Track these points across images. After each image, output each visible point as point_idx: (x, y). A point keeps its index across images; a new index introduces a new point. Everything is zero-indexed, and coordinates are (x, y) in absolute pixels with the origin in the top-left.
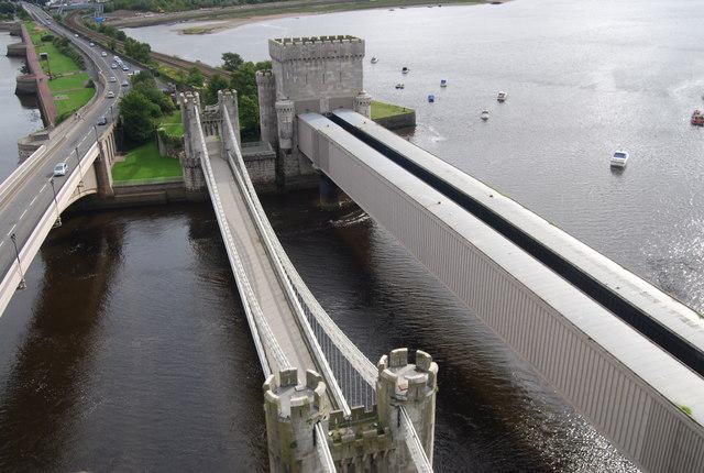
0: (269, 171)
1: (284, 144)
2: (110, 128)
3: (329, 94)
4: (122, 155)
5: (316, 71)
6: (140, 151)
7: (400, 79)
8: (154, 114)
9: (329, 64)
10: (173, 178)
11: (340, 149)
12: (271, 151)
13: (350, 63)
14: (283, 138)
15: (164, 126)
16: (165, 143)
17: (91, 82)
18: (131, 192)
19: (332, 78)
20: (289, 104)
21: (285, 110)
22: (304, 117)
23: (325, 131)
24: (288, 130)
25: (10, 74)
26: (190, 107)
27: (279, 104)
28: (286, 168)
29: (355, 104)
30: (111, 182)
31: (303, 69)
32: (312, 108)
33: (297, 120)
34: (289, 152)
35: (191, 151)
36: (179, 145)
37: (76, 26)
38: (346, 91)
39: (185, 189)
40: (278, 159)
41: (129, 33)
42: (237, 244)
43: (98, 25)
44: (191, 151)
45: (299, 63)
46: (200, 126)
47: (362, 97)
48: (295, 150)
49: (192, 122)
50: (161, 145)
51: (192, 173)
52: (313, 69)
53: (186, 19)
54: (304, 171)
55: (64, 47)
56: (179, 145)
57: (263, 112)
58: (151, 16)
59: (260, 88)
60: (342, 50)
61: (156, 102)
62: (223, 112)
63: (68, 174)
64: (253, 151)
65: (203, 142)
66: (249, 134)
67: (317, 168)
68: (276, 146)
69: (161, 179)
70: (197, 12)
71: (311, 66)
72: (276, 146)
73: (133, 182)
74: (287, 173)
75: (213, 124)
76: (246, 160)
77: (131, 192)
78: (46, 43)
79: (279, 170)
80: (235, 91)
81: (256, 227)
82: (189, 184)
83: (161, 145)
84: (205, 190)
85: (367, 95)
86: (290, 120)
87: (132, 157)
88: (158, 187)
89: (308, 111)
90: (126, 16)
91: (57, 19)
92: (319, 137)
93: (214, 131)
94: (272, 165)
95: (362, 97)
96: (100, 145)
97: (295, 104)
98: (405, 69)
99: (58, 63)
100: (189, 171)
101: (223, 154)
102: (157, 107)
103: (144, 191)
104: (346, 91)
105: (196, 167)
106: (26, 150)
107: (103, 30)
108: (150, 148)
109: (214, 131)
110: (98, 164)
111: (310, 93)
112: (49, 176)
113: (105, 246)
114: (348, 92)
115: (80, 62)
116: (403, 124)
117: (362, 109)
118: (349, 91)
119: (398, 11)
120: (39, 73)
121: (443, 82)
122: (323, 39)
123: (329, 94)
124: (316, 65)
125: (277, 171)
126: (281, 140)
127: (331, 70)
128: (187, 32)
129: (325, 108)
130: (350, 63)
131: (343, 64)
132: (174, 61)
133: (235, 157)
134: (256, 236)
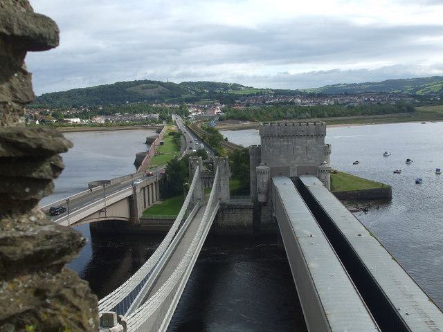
5: (288, 145)
7: (402, 166)
18: (151, 224)
19: (300, 151)
21: (262, 173)
24: (264, 188)
29: (317, 172)
30: (140, 215)
32: (283, 173)
33: (270, 185)
34: (265, 204)
38: (311, 161)
40: (258, 208)
52: (286, 143)
58: (248, 123)
59: (251, 157)
68: (256, 198)
71: (284, 141)
74: (262, 220)
75: (207, 179)
77: (151, 224)
79: (257, 217)
86: (265, 181)
87: (167, 202)
89: (280, 175)
90: (230, 123)
94: (251, 213)
95: (322, 166)
96: (134, 189)
98: (408, 160)
103: (159, 224)
104: (311, 161)
110: (131, 200)
111: (282, 161)
117: (323, 176)
118: (314, 161)
119: (429, 124)
121: (438, 170)
124: (288, 141)
131: (309, 141)
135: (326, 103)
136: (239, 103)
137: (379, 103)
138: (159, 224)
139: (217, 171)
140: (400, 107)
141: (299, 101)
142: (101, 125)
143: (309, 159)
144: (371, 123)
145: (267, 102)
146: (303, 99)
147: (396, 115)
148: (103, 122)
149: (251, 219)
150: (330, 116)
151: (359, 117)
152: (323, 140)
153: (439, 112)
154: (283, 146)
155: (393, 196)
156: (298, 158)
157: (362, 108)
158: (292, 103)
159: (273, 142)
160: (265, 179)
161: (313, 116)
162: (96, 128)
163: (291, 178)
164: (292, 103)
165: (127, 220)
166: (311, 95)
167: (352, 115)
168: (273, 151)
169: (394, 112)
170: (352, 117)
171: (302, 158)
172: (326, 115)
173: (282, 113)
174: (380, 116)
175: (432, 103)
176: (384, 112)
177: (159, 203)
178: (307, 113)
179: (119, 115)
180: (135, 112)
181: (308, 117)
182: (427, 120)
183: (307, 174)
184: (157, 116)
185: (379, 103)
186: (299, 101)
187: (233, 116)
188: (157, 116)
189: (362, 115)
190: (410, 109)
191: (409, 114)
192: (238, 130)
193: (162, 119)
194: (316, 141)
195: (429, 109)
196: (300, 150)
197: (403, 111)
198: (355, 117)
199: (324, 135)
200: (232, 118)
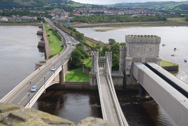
0: (120, 82)
1: (127, 73)
2: (67, 61)
3: (145, 56)
4: (70, 71)
5: (142, 47)
6: (76, 70)
8: (82, 58)
9: (147, 45)
10: (86, 81)
11: (148, 76)
12: (122, 75)
13: (154, 45)
14: (127, 70)
15: (85, 62)
16: (85, 68)
17: (63, 45)
18: (71, 84)
20: (131, 58)
21: (129, 60)
22: (135, 64)
23: (143, 69)
24: (129, 68)
25: (37, 40)
26: (95, 56)
27: (127, 58)
28: (127, 82)
29: (155, 60)
30: (64, 80)
31: (137, 46)
32: (139, 60)
34: (129, 76)
35: (93, 72)
36: (89, 69)
37: (60, 26)
39: (90, 85)
40: (125, 78)
41: (78, 30)
42: (105, 106)
43: (67, 26)
44: (93, 72)
45: (136, 44)
46: (98, 64)
47: (158, 58)
48: (131, 75)
49: (95, 62)
50: (83, 69)
51: (93, 80)
52: (141, 46)
53: (98, 26)
54: (134, 83)
55: (55, 33)
56: (89, 69)
57: (121, 60)
58: (86, 24)
59: (121, 52)
60: (152, 40)
61: (83, 54)
62: (106, 59)
63: (37, 90)
64: (115, 74)
65: (98, 69)
66: (115, 68)
67: (139, 83)
68: (124, 73)
69: (81, 81)
70: (103, 24)
71: (140, 45)
72: (124, 73)
73: (72, 81)
74: (127, 83)
75: (102, 63)
76: (113, 77)
77: (71, 84)
78: (50, 31)
79: (124, 82)
80: (111, 52)
81: (114, 102)
82: (91, 84)
83: (83, 69)
84: (97, 86)
85: (160, 58)
86: (130, 64)
87: (72, 72)
88: (81, 84)
89: (137, 61)
91: (55, 23)
92: (140, 71)
93: (102, 66)
94: (122, 80)
95: (158, 58)
96: (62, 67)
97: (133, 58)
98: (175, 49)
99: (53, 38)
100: (92, 79)
101: (105, 74)
102: (84, 56)
103: (75, 85)
104: (152, 55)
105: (95, 78)
106: (38, 66)
107: (69, 28)
108: (79, 69)
109: (102, 66)
110: (61, 73)
111: (139, 55)
112: (28, 91)
113: (59, 102)
114: (153, 56)
115: (59, 38)
116: (174, 69)
117: (158, 63)
119: (175, 27)
120: (46, 42)
122: (145, 36)
123: (145, 56)
124: (142, 45)
125: (123, 82)
126: (126, 71)
127: (147, 47)
128: (97, 31)
129: (144, 61)
130: (154, 45)
131: (152, 46)
132: (92, 40)
133: (109, 76)
134: (113, 105)
135: (120, 13)
136: (75, 12)
137: (147, 15)
138: (75, 85)
139: (107, 59)
140: (159, 18)
141: (106, 12)
142: (7, 22)
143: (151, 54)
144: (147, 26)
145: (90, 12)
146: (108, 11)
147: (158, 22)
148: (7, 20)
149: (122, 83)
150: (126, 21)
151: (140, 22)
152: (159, 45)
153: (178, 21)
154: (140, 47)
155: (179, 69)
156: (146, 54)
157: (141, 18)
158: (103, 13)
159: (135, 45)
160: (130, 63)
161: (118, 22)
162: (4, 24)
163: (143, 63)
164: (103, 13)
165: (58, 83)
166: (111, 9)
167: (137, 21)
168: (134, 50)
169: (157, 20)
170: (137, 23)
171: (148, 54)
172: (124, 20)
173: (102, 19)
174: (150, 22)
175: (173, 16)
176: (152, 20)
177: (69, 72)
178: (114, 20)
179: (14, 16)
180: (22, 15)
181: (115, 22)
182: (174, 26)
183: (150, 61)
184: (36, 18)
185: (147, 15)
186: (106, 12)
187: (77, 20)
188: (36, 18)
189: (142, 21)
190: (164, 20)
191: (163, 22)
192: (82, 28)
193: (39, 20)
194: (156, 46)
195: (173, 19)
196: (147, 50)
197: (161, 20)
198: (138, 23)
199: (159, 43)
200: (76, 21)
